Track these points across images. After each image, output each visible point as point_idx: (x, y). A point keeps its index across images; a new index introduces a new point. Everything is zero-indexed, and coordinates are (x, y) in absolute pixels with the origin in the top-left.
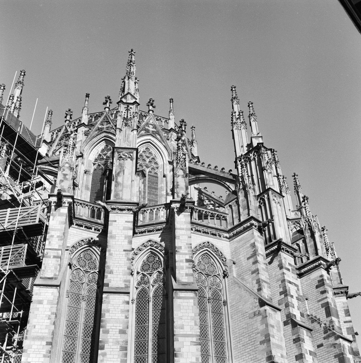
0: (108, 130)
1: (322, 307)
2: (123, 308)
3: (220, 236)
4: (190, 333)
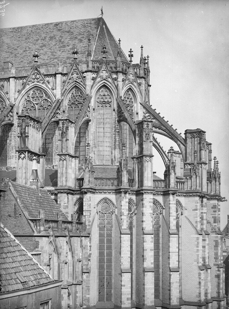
0: (107, 78)
1: (213, 218)
2: (151, 240)
3: (181, 195)
4: (175, 251)
